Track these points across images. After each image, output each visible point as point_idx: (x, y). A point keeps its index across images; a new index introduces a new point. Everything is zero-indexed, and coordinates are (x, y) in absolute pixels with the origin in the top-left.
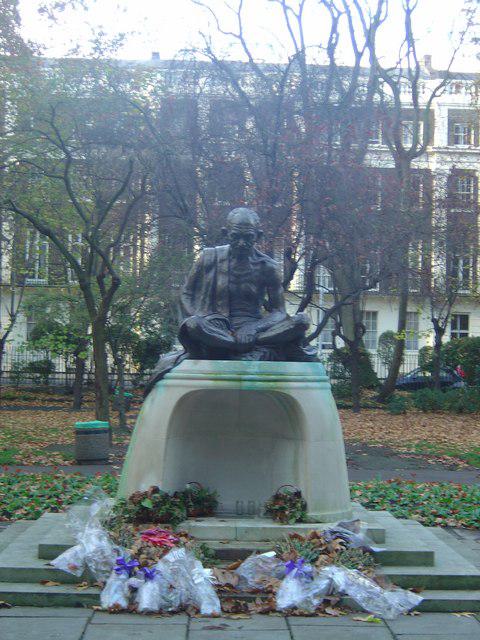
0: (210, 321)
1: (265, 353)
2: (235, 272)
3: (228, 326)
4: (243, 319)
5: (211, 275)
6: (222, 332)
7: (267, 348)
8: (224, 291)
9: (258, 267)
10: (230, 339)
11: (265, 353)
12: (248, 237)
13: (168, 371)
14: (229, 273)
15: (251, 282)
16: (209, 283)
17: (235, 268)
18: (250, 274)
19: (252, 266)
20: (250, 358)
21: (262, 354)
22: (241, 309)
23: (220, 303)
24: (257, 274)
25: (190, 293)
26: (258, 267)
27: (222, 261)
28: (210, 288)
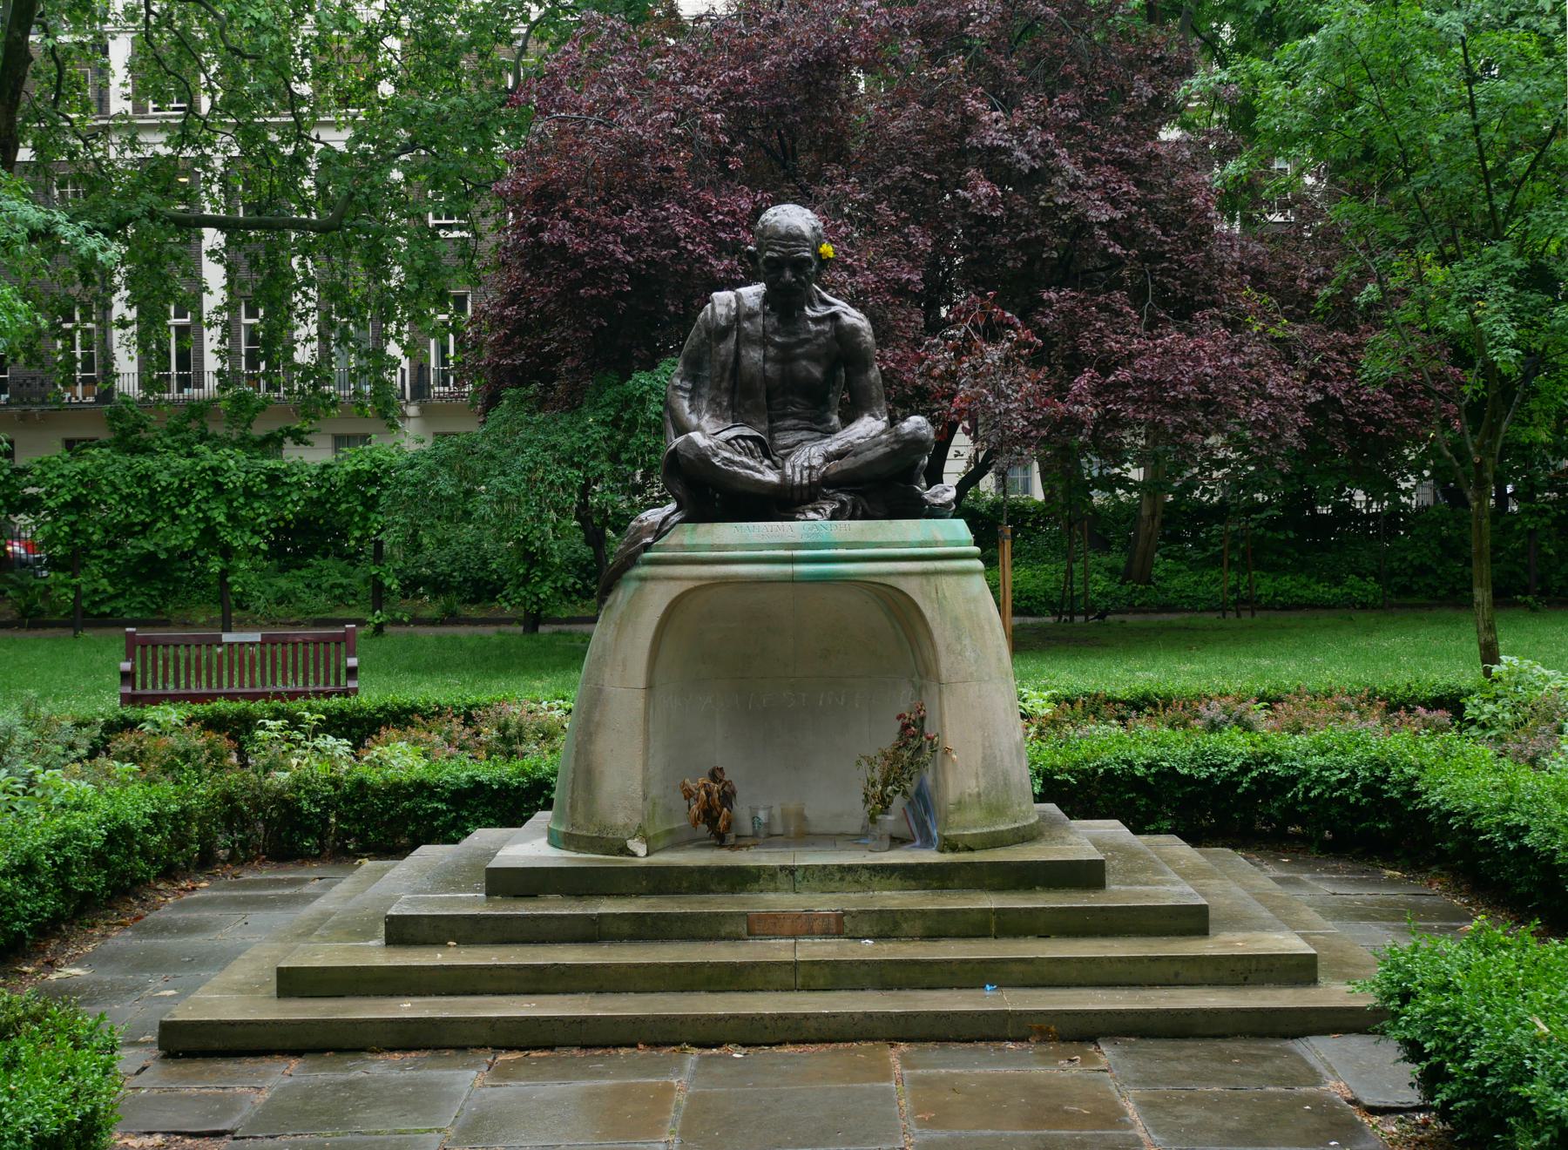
0: (728, 442)
1: (843, 503)
3: (766, 449)
4: (800, 436)
5: (730, 344)
6: (752, 463)
9: (826, 327)
10: (772, 477)
11: (843, 503)
12: (800, 265)
13: (647, 547)
14: (764, 341)
16: (724, 366)
18: (807, 341)
19: (812, 326)
20: (811, 515)
22: (794, 415)
24: (822, 340)
25: (688, 385)
26: (826, 327)
28: (727, 375)
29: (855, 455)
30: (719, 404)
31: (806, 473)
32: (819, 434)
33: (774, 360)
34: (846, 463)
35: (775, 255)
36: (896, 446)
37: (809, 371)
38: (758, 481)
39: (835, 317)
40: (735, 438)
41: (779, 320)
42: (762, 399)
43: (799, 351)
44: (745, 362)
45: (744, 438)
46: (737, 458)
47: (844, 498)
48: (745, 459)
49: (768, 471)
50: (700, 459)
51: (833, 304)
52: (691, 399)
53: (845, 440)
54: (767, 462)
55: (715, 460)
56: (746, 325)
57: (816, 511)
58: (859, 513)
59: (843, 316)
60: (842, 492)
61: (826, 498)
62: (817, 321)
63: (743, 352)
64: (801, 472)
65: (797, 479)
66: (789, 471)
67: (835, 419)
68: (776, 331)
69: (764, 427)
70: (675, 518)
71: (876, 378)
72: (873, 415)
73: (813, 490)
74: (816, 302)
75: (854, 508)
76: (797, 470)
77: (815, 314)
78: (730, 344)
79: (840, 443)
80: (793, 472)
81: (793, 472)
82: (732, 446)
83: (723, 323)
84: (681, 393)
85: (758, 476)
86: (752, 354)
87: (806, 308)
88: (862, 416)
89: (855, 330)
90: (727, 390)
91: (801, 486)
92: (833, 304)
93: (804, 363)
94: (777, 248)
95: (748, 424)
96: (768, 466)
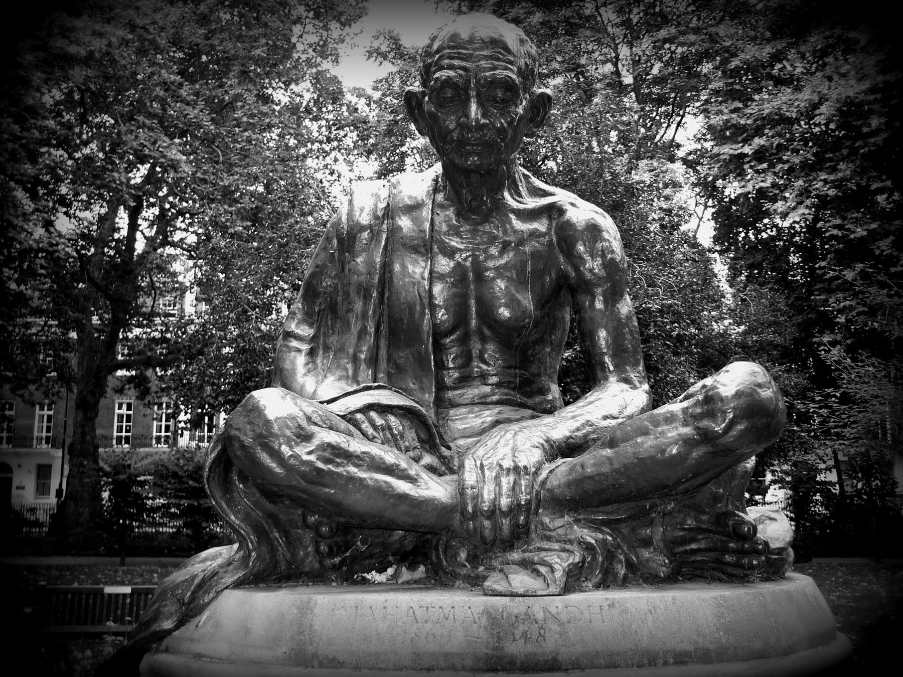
0: (349, 418)
6: (390, 456)
7: (596, 526)
19: (519, 225)
20: (521, 580)
25: (306, 331)
26: (541, 226)
27: (413, 208)
29: (612, 443)
31: (507, 482)
32: (529, 412)
35: (451, 73)
38: (404, 497)
39: (554, 211)
40: (366, 409)
41: (458, 214)
45: (383, 409)
46: (357, 446)
48: (375, 450)
49: (425, 476)
51: (551, 194)
52: (312, 353)
53: (581, 421)
54: (428, 459)
56: (405, 223)
63: (397, 267)
64: (497, 478)
65: (488, 494)
66: (470, 477)
67: (555, 391)
69: (430, 397)
71: (629, 318)
72: (627, 381)
74: (523, 191)
75: (610, 556)
76: (490, 474)
77: (522, 206)
79: (575, 425)
82: (357, 425)
84: (294, 343)
85: (402, 486)
92: (551, 194)
94: (456, 62)
95: (392, 384)
96: (431, 469)
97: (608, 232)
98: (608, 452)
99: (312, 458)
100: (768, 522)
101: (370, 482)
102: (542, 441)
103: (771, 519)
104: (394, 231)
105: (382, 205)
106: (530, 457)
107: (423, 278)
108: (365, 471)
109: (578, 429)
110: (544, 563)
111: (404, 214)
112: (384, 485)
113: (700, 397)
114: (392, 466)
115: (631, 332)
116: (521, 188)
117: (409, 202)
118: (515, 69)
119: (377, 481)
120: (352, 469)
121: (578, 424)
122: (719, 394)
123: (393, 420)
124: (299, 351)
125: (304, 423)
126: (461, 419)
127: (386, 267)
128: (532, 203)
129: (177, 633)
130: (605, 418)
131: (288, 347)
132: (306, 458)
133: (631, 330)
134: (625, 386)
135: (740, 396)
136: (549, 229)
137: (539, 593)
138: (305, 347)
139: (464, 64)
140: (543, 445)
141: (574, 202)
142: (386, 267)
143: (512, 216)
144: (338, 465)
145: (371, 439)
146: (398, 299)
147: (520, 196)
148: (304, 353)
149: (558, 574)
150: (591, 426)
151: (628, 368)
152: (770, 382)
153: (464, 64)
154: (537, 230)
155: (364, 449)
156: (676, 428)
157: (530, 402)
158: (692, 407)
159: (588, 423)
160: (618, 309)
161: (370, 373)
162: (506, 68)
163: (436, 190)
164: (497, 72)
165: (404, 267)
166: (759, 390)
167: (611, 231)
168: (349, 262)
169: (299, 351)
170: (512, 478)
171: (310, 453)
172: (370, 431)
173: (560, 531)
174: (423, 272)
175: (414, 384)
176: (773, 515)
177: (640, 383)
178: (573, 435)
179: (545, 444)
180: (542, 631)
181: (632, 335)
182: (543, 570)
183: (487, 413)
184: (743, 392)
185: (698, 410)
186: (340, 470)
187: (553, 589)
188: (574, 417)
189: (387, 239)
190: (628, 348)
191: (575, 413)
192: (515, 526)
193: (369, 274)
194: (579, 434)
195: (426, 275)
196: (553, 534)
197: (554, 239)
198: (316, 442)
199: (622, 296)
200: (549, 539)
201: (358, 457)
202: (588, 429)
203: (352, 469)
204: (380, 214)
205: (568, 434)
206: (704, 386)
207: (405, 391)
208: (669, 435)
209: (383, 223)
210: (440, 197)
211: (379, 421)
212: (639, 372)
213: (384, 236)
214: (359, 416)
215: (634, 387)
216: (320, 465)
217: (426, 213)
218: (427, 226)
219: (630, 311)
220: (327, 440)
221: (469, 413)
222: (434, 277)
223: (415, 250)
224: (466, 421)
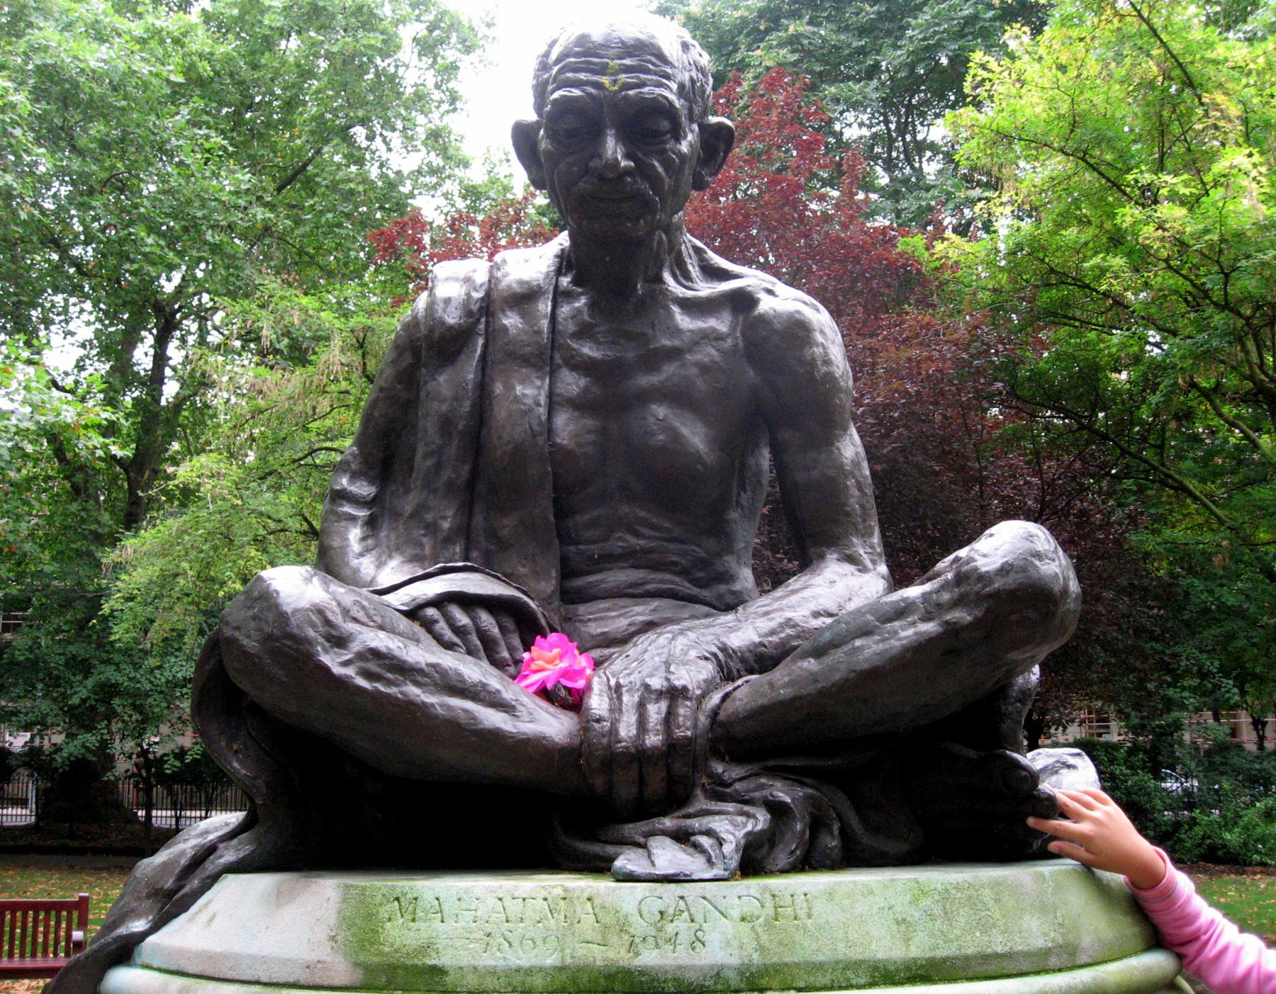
0: (414, 613)
1: (777, 810)
2: (588, 350)
4: (640, 612)
5: (468, 370)
8: (519, 453)
11: (777, 810)
15: (679, 397)
16: (446, 423)
17: (584, 332)
18: (674, 354)
19: (684, 321)
20: (667, 856)
21: (761, 820)
22: (631, 558)
23: (507, 525)
24: (709, 353)
25: (364, 489)
26: (720, 323)
27: (524, 298)
29: (819, 652)
30: (432, 528)
31: (656, 711)
32: (706, 609)
33: (579, 405)
34: (780, 683)
35: (576, 92)
36: (961, 616)
37: (676, 436)
38: (495, 737)
39: (742, 302)
40: (441, 601)
41: (592, 305)
42: (544, 507)
43: (645, 380)
44: (500, 413)
46: (421, 653)
47: (782, 793)
48: (450, 661)
50: (277, 654)
52: (372, 524)
53: (778, 618)
55: (332, 661)
56: (511, 321)
57: (682, 837)
58: (831, 842)
59: (762, 296)
60: (775, 772)
61: (720, 792)
62: (694, 307)
63: (498, 388)
64: (641, 706)
66: (598, 703)
67: (746, 577)
68: (584, 332)
69: (548, 586)
70: (228, 855)
71: (856, 464)
72: (852, 559)
73: (679, 768)
74: (694, 271)
75: (817, 825)
77: (690, 294)
78: (468, 370)
79: (765, 625)
80: (616, 707)
81: (616, 707)
82: (428, 625)
83: (452, 318)
84: (347, 509)
85: (492, 718)
86: (519, 389)
87: (667, 277)
88: (822, 557)
89: (798, 330)
90: (450, 485)
91: (640, 757)
93: (661, 411)
95: (487, 566)
97: (822, 332)
98: (810, 664)
99: (350, 671)
100: (1064, 771)
101: (440, 711)
102: (715, 650)
103: (1069, 767)
104: (493, 333)
105: (477, 295)
106: (693, 674)
107: (539, 405)
108: (432, 693)
109: (773, 632)
110: (709, 833)
111: (511, 308)
112: (462, 715)
113: (950, 576)
114: (475, 685)
115: (860, 487)
116: (690, 268)
117: (519, 290)
118: (674, 86)
119: (449, 708)
120: (413, 691)
121: (773, 624)
122: (976, 569)
123: (486, 619)
124: (353, 519)
125: (337, 619)
126: (596, 620)
127: (483, 389)
128: (706, 289)
129: (151, 939)
130: (816, 615)
131: (337, 513)
132: (337, 670)
133: (858, 483)
134: (848, 568)
135: (1008, 572)
136: (733, 328)
137: (695, 877)
138: (362, 513)
139: (595, 78)
140: (715, 655)
141: (770, 287)
142: (483, 389)
143: (676, 309)
144: (389, 683)
145: (449, 646)
146: (500, 437)
147: (687, 276)
148: (360, 523)
149: (728, 848)
150: (794, 626)
151: (855, 540)
152: (1055, 551)
153: (595, 78)
154: (714, 330)
155: (433, 659)
156: (913, 624)
157: (705, 593)
158: (938, 591)
159: (789, 623)
160: (838, 449)
161: (458, 550)
162: (661, 85)
163: (559, 272)
164: (646, 89)
165: (509, 388)
166: (1037, 563)
167: (828, 331)
168: (426, 383)
169: (353, 519)
170: (663, 705)
171: (346, 664)
172: (449, 635)
173: (737, 786)
174: (539, 395)
175: (524, 566)
176: (1072, 761)
177: (874, 562)
178: (765, 640)
179: (720, 655)
180: (699, 934)
181: (860, 489)
182: (705, 841)
183: (638, 609)
184: (1011, 565)
185: (946, 596)
186: (392, 690)
187: (718, 871)
188: (767, 613)
189: (486, 346)
190: (854, 509)
191: (769, 608)
192: (671, 780)
193: (456, 398)
194: (774, 639)
195: (543, 400)
196: (728, 790)
197: (741, 343)
198: (356, 647)
199: (845, 429)
200: (722, 798)
201: (421, 671)
202: (789, 631)
203: (413, 691)
204: (475, 308)
205: (757, 639)
206: (957, 559)
207: (508, 578)
208: (903, 634)
209: (478, 321)
210: (565, 281)
211: (462, 618)
212: (872, 547)
213: (481, 341)
214: (431, 612)
215: (864, 570)
216: (362, 682)
217: (545, 306)
218: (545, 324)
219: (857, 453)
220: (373, 644)
221: (608, 610)
222: (553, 402)
223: (526, 361)
224: (602, 623)
